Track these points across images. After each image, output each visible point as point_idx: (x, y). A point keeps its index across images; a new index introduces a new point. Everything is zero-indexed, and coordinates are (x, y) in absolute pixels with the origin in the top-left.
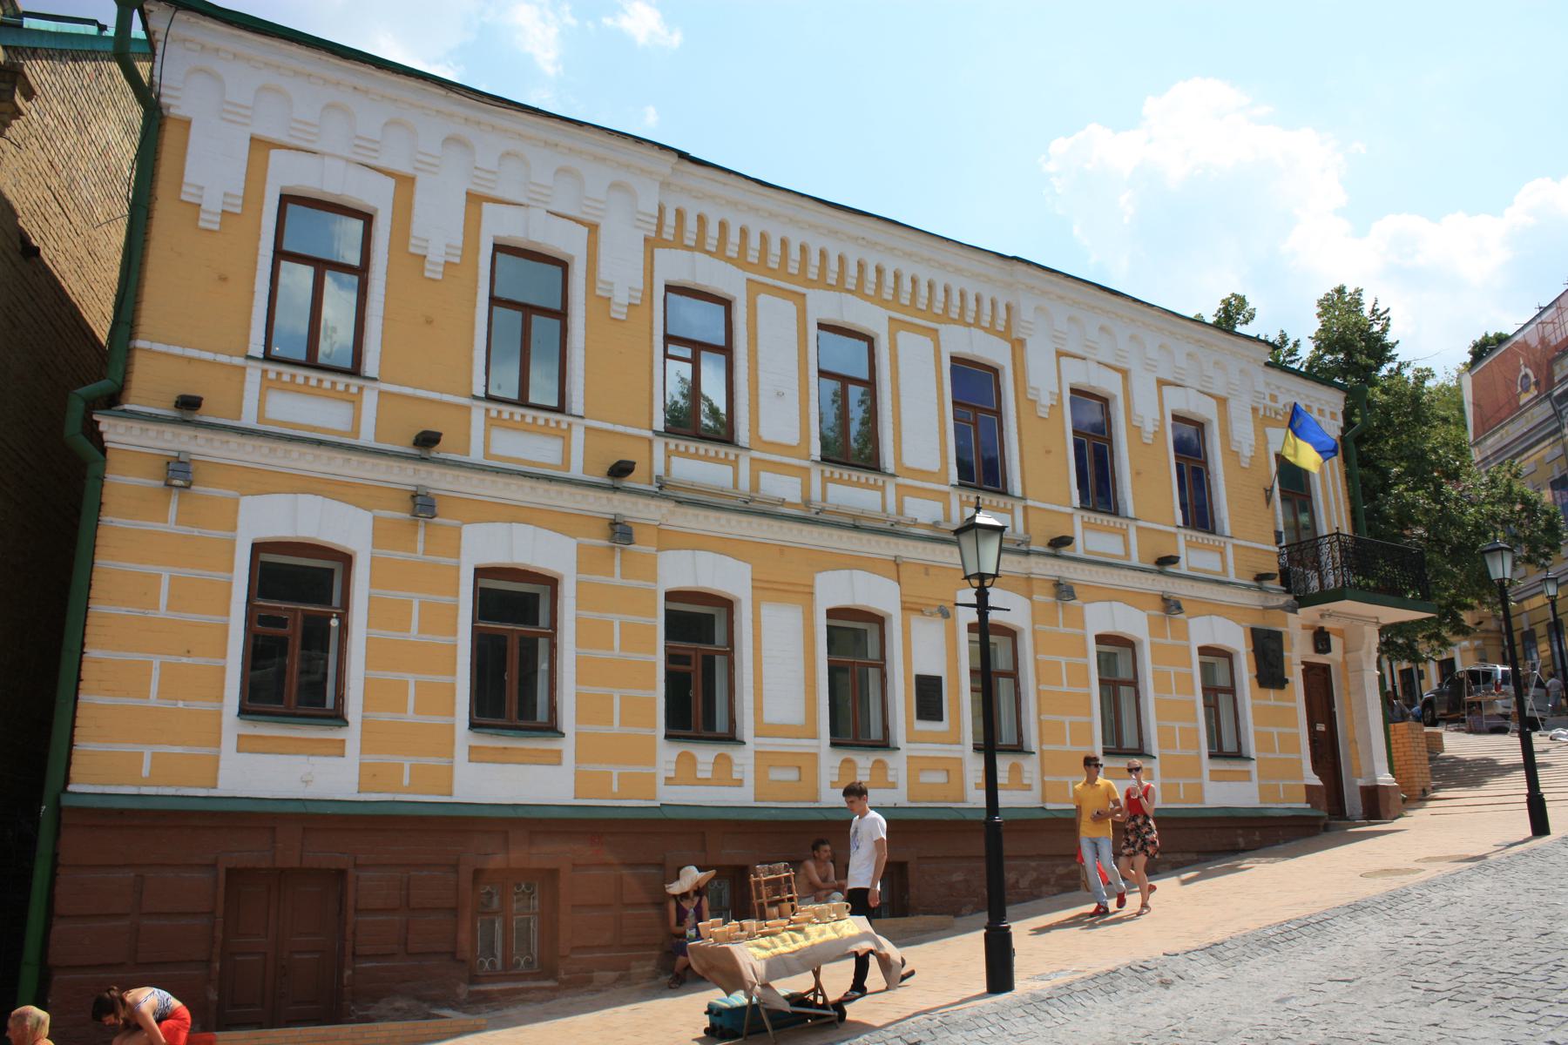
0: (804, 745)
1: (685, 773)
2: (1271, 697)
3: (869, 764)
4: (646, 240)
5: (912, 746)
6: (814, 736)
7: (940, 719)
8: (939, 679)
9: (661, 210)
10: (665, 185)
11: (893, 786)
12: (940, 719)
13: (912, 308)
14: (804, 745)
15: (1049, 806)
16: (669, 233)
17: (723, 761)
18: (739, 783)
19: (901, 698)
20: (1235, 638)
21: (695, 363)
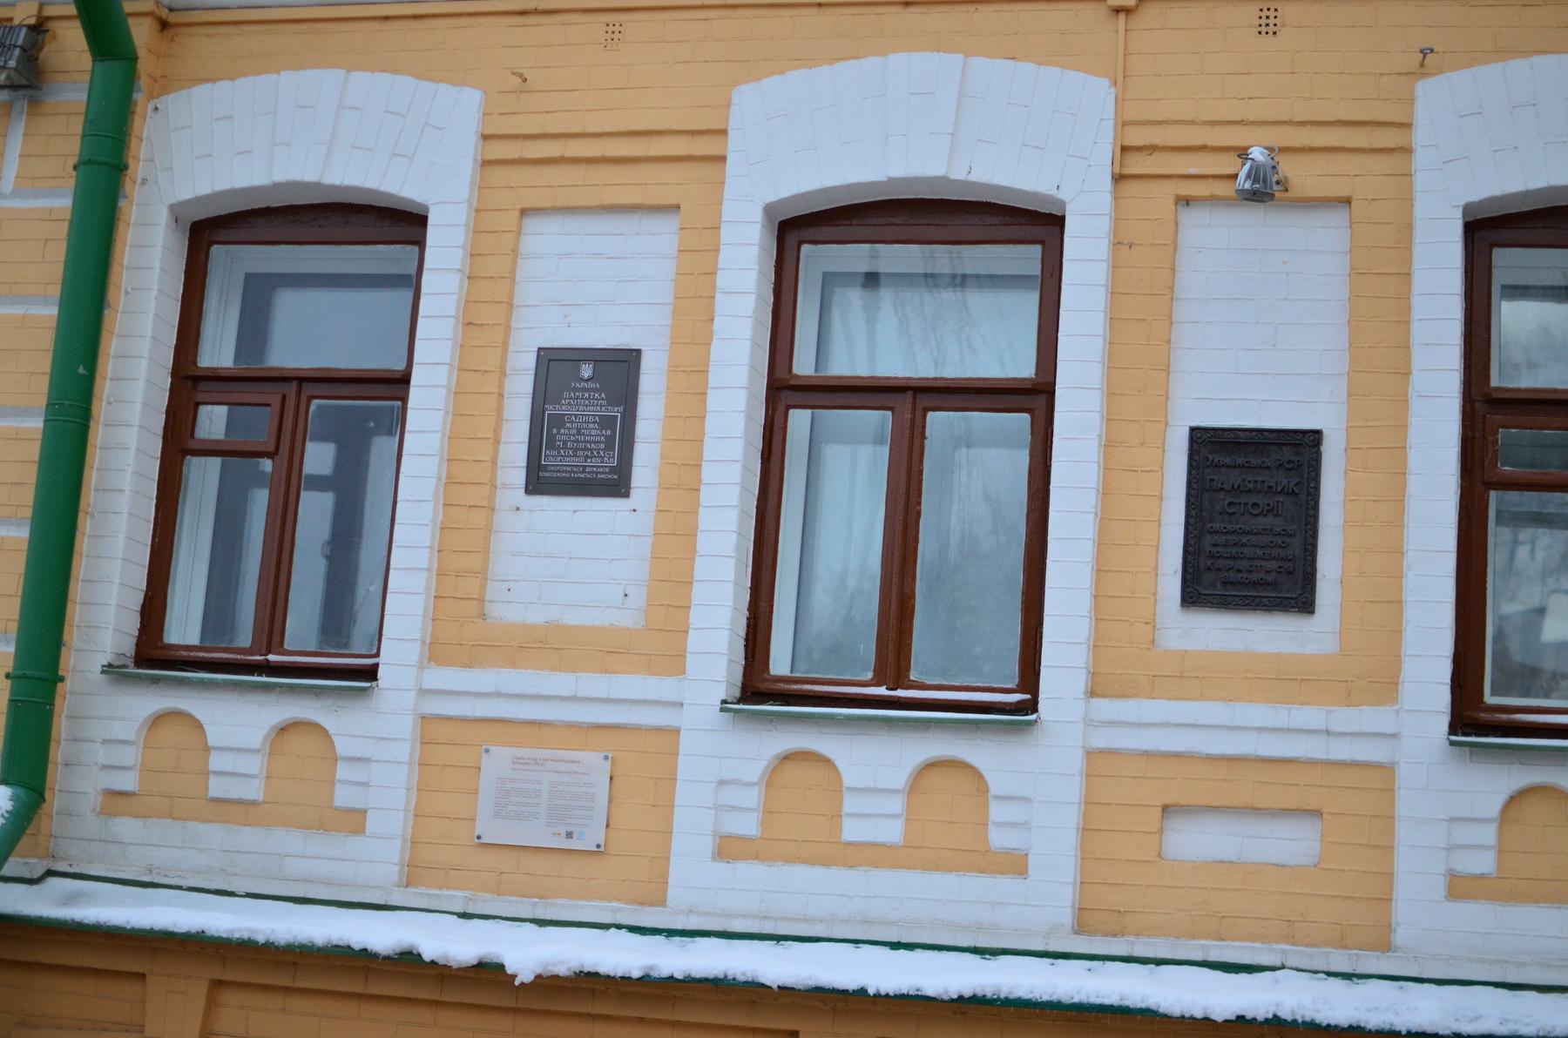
0: (626, 693)
3: (899, 776)
5: (1106, 708)
6: (673, 662)
7: (1303, 602)
8: (1305, 444)
11: (1016, 864)
12: (1303, 602)
14: (626, 693)
18: (354, 821)
19: (1115, 514)
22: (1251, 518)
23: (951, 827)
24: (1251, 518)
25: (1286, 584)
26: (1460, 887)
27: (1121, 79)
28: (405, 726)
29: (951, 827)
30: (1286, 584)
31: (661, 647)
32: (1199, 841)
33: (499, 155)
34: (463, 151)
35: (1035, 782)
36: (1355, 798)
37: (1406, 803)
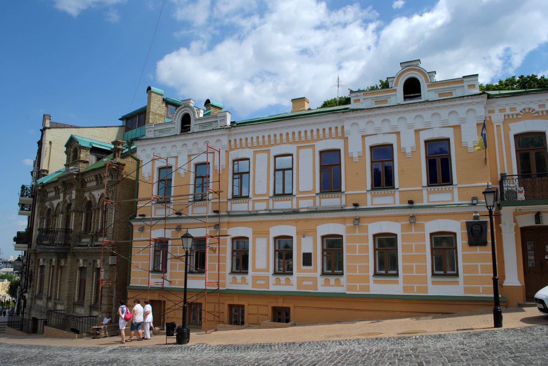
0: (265, 274)
1: (235, 281)
2: (478, 250)
4: (226, 151)
7: (311, 265)
8: (310, 254)
9: (230, 141)
10: (229, 135)
12: (311, 265)
13: (300, 141)
14: (265, 274)
15: (347, 293)
16: (233, 147)
17: (243, 279)
20: (456, 227)
21: (241, 178)
22: (307, 259)
23: (288, 283)
24: (307, 259)
25: (310, 264)
26: (322, 285)
27: (296, 227)
28: (251, 277)
29: (288, 283)
30: (310, 264)
31: (267, 270)
32: (305, 283)
33: (254, 233)
34: (251, 233)
35: (293, 279)
36: (315, 280)
37: (318, 280)
